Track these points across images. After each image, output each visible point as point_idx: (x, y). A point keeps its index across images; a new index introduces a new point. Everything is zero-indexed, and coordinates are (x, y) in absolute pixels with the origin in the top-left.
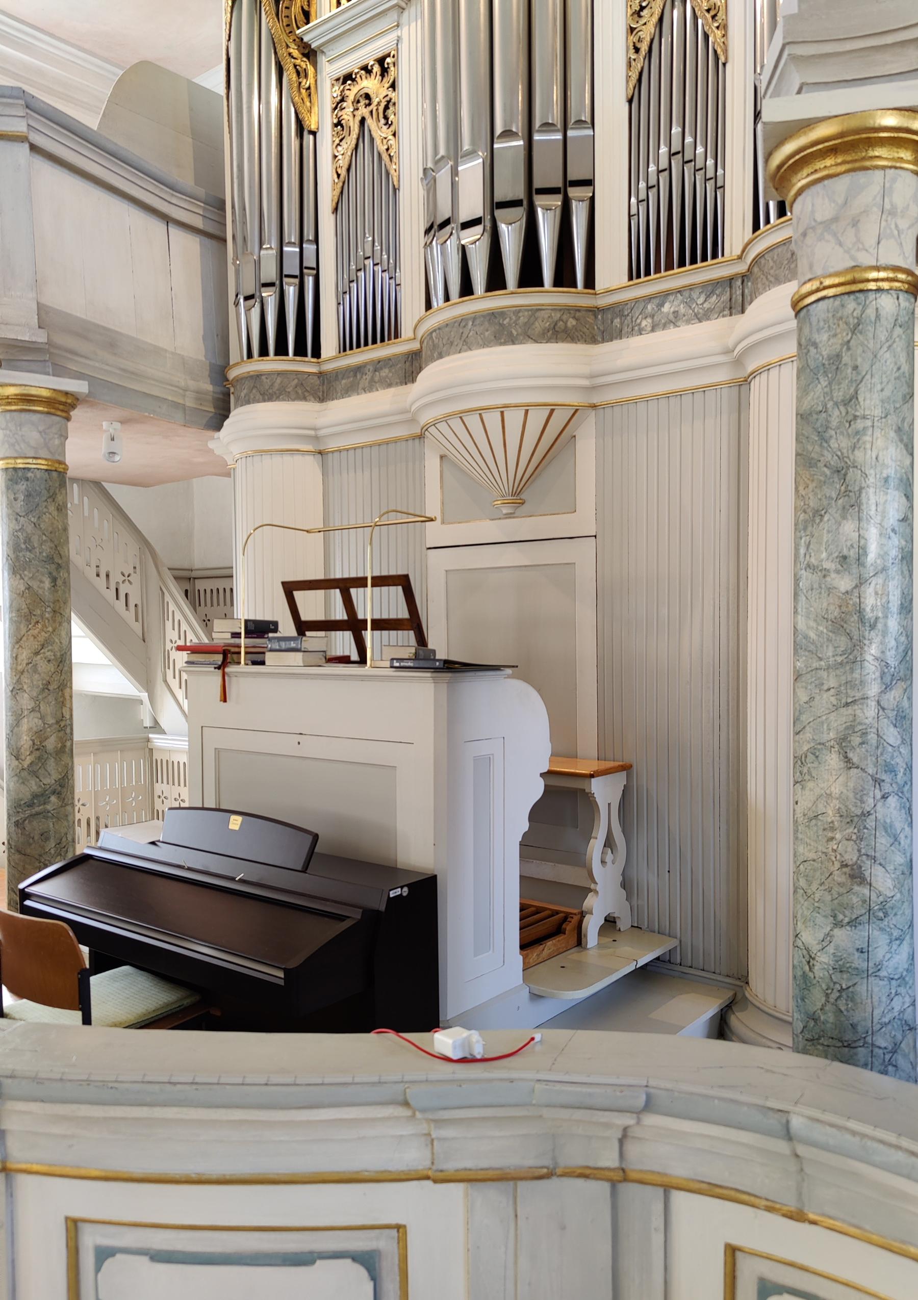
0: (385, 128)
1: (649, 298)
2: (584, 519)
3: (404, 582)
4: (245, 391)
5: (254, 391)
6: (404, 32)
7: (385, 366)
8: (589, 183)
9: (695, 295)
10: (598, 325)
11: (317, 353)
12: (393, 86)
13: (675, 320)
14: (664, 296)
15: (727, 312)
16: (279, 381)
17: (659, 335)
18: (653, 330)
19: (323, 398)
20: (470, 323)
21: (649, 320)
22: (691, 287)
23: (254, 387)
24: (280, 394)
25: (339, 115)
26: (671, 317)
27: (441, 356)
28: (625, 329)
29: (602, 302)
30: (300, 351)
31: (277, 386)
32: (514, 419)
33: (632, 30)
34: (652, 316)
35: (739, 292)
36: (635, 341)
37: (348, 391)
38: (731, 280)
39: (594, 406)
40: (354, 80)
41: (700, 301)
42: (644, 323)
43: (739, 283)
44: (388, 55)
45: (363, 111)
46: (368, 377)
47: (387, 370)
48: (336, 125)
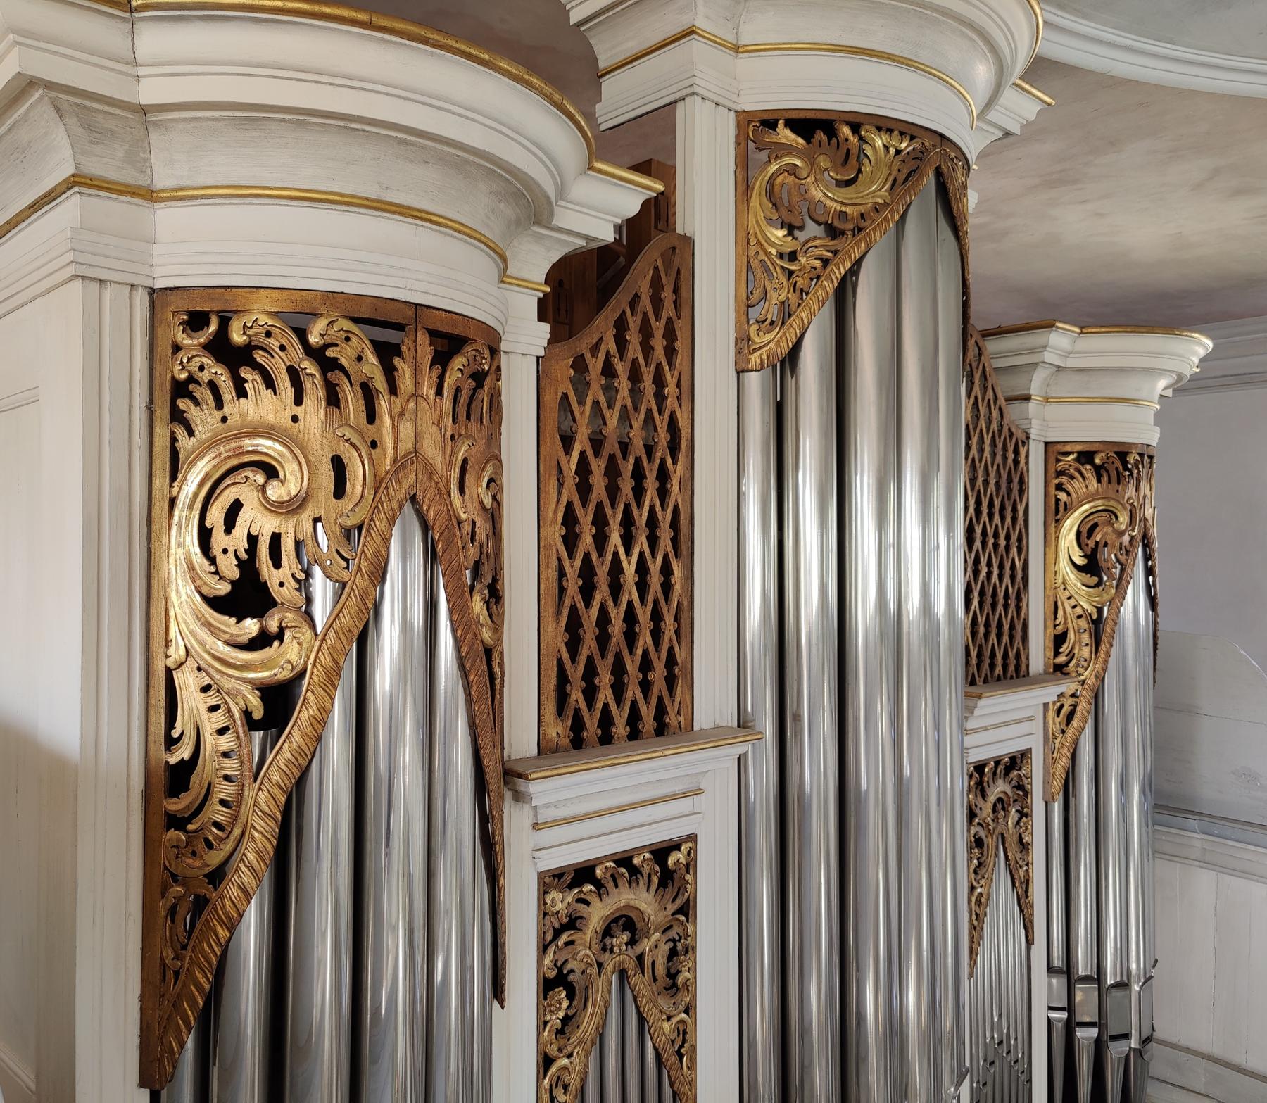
44: (676, 847)
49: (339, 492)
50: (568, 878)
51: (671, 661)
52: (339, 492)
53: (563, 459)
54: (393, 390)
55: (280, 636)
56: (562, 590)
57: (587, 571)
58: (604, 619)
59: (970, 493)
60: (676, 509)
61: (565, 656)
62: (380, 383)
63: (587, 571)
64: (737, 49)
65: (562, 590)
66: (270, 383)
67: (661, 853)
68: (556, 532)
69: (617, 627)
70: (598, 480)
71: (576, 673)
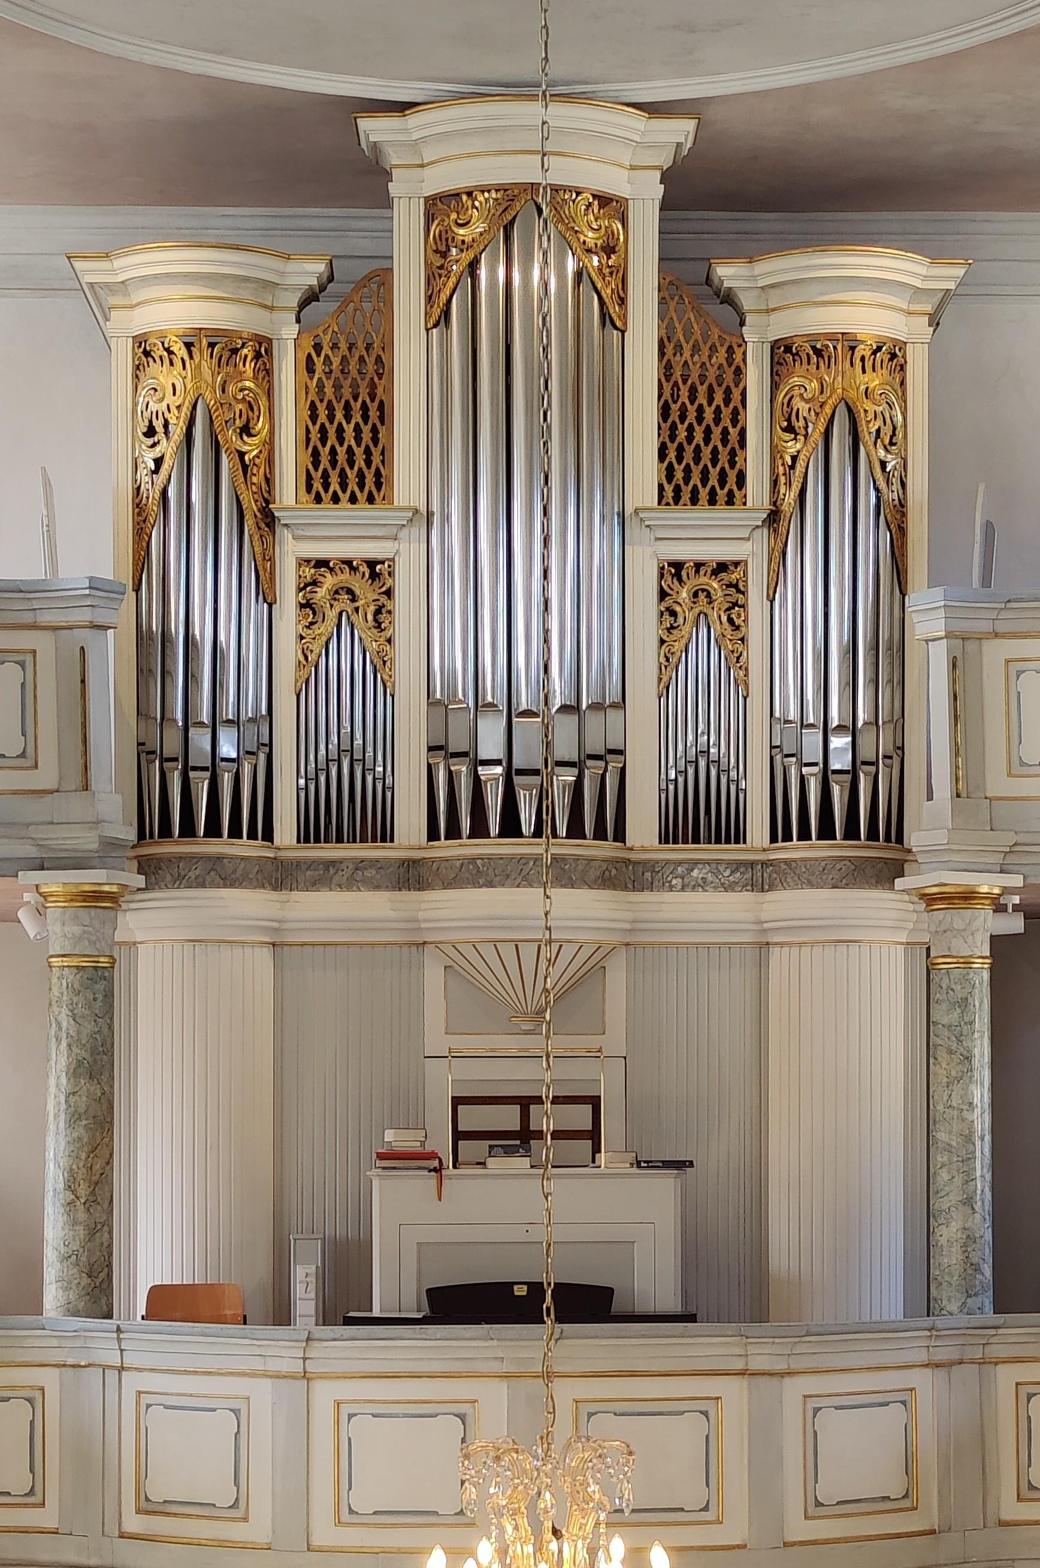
0: (375, 631)
1: (680, 863)
2: (615, 1040)
3: (595, 1102)
4: (197, 872)
5: (212, 873)
6: (403, 547)
7: (371, 867)
8: (621, 752)
9: (721, 868)
10: (628, 876)
11: (268, 836)
12: (389, 593)
13: (702, 885)
14: (694, 864)
15: (749, 888)
16: (242, 866)
17: (688, 896)
18: (683, 889)
19: (278, 886)
20: (532, 863)
21: (680, 880)
22: (718, 862)
23: (212, 869)
24: (243, 881)
25: (309, 596)
26: (700, 881)
27: (490, 884)
28: (656, 883)
29: (633, 856)
30: (252, 835)
31: (239, 871)
32: (568, 951)
33: (662, 642)
34: (683, 879)
35: (760, 874)
36: (668, 896)
37: (314, 885)
38: (752, 864)
39: (627, 944)
40: (331, 570)
41: (727, 874)
42: (674, 882)
43: (759, 867)
44: (383, 563)
45: (344, 602)
46: (347, 873)
47: (374, 872)
48: (302, 606)
49: (174, 394)
50: (313, 563)
51: (378, 474)
52: (174, 394)
53: (309, 382)
54: (191, 357)
55: (159, 442)
56: (308, 440)
57: (323, 430)
58: (333, 452)
59: (665, 384)
60: (382, 403)
61: (311, 467)
62: (186, 358)
63: (323, 430)
64: (422, 166)
65: (308, 440)
66: (155, 361)
67: (372, 564)
68: (306, 413)
69: (342, 456)
70: (329, 391)
71: (317, 475)
